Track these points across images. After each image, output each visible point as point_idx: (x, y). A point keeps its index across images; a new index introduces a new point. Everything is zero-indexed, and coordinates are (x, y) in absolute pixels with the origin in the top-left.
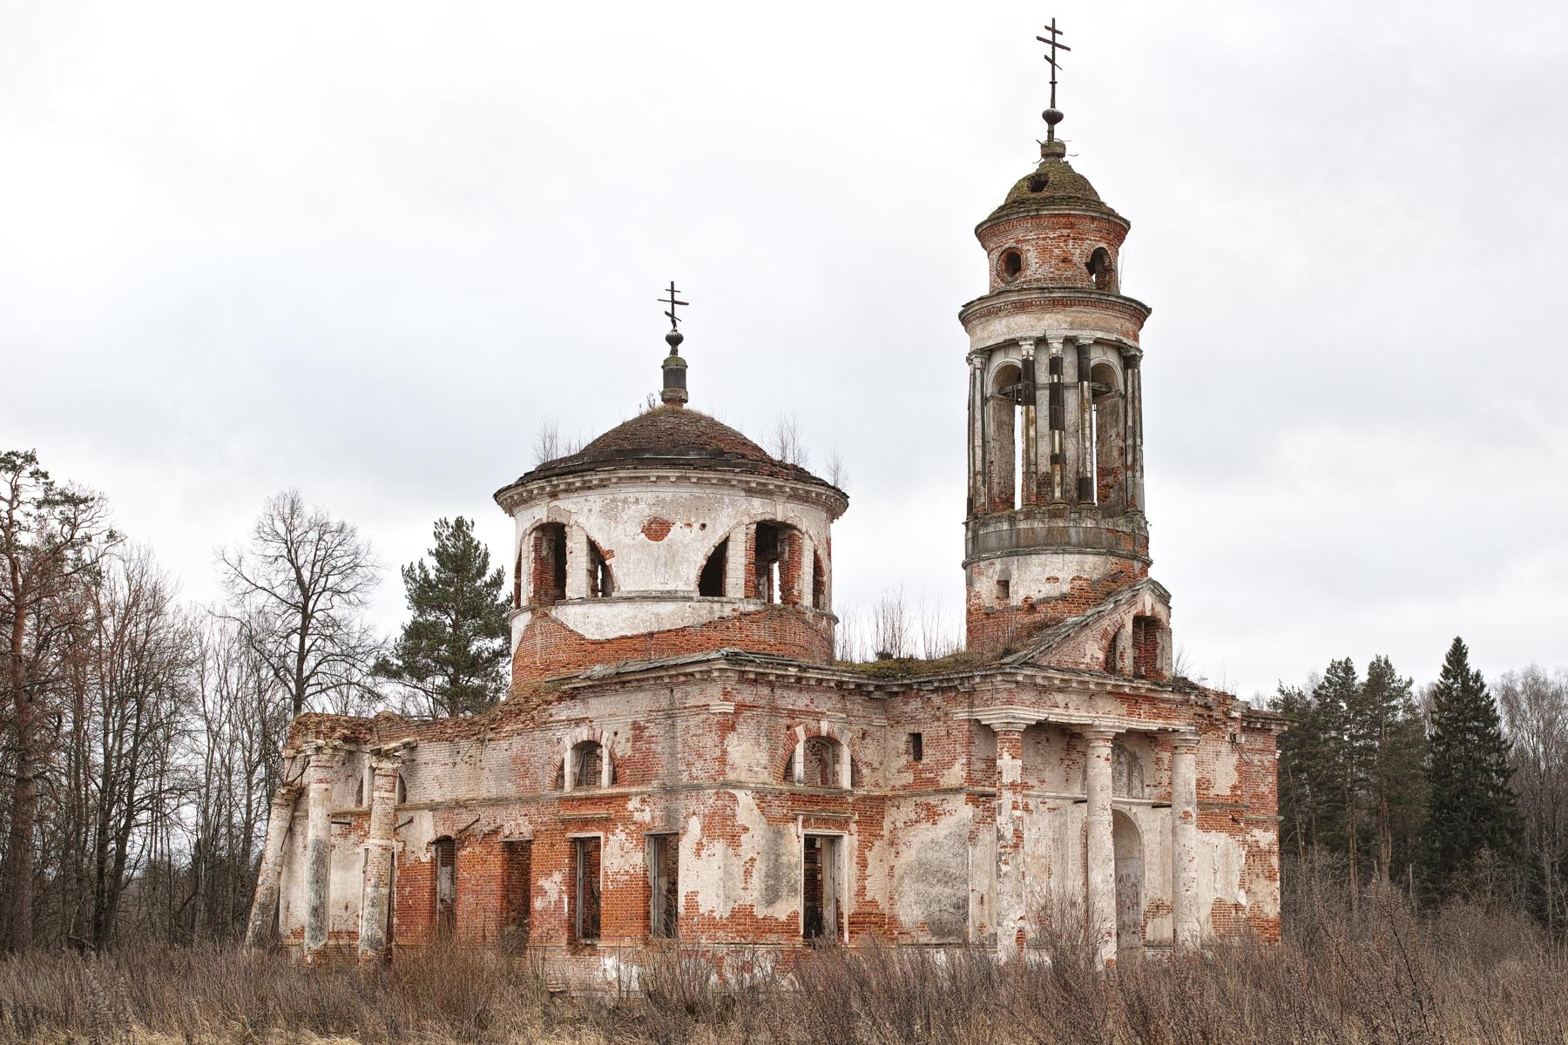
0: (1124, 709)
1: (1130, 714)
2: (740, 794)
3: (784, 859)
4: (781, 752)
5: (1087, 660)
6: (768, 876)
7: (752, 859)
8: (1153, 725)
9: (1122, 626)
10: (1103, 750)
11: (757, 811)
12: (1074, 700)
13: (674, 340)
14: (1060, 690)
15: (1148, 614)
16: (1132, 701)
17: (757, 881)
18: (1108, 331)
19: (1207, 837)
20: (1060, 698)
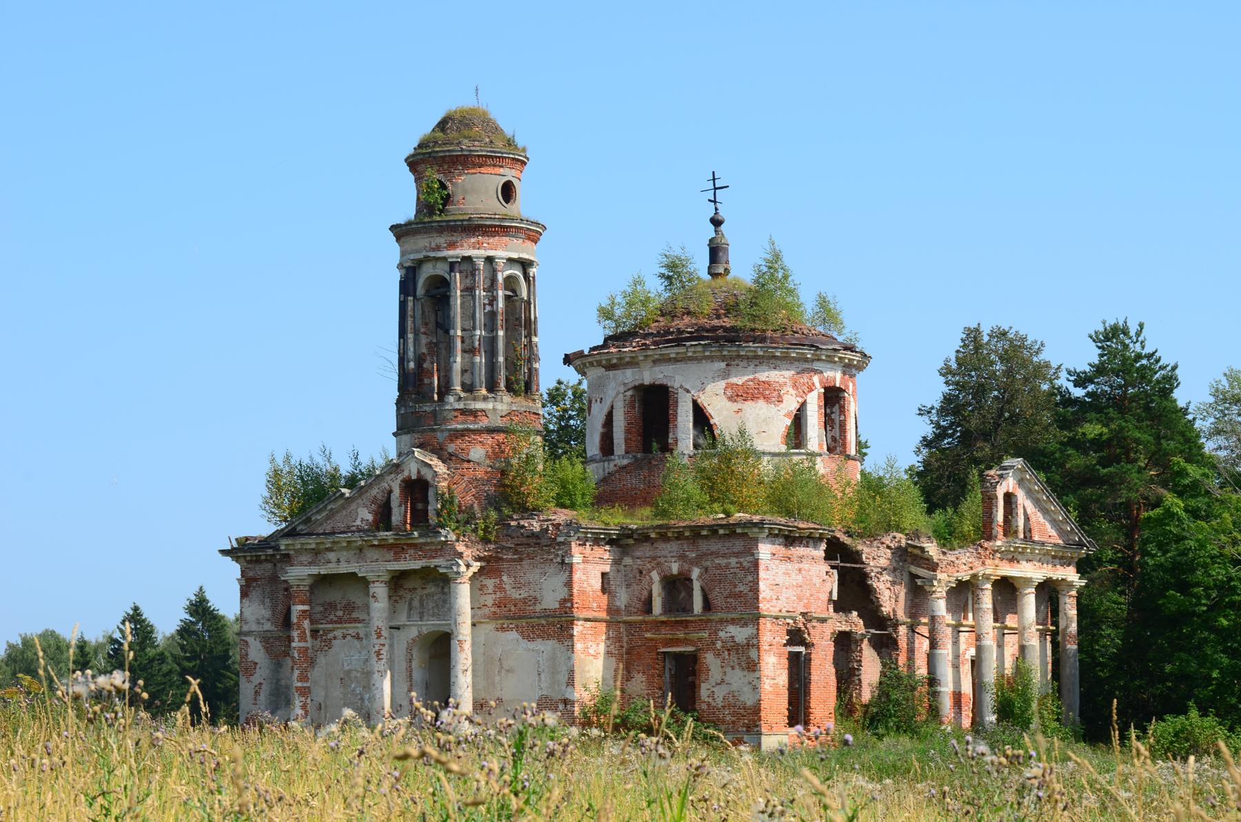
0: (390, 555)
1: (395, 560)
2: (250, 640)
3: (283, 682)
4: (280, 607)
5: (358, 522)
6: (271, 694)
7: (260, 684)
8: (416, 565)
9: (390, 492)
10: (380, 591)
11: (262, 651)
12: (344, 555)
13: (716, 222)
14: (330, 550)
15: (414, 477)
16: (398, 549)
17: (262, 698)
18: (418, 251)
19: (531, 645)
20: (332, 556)
